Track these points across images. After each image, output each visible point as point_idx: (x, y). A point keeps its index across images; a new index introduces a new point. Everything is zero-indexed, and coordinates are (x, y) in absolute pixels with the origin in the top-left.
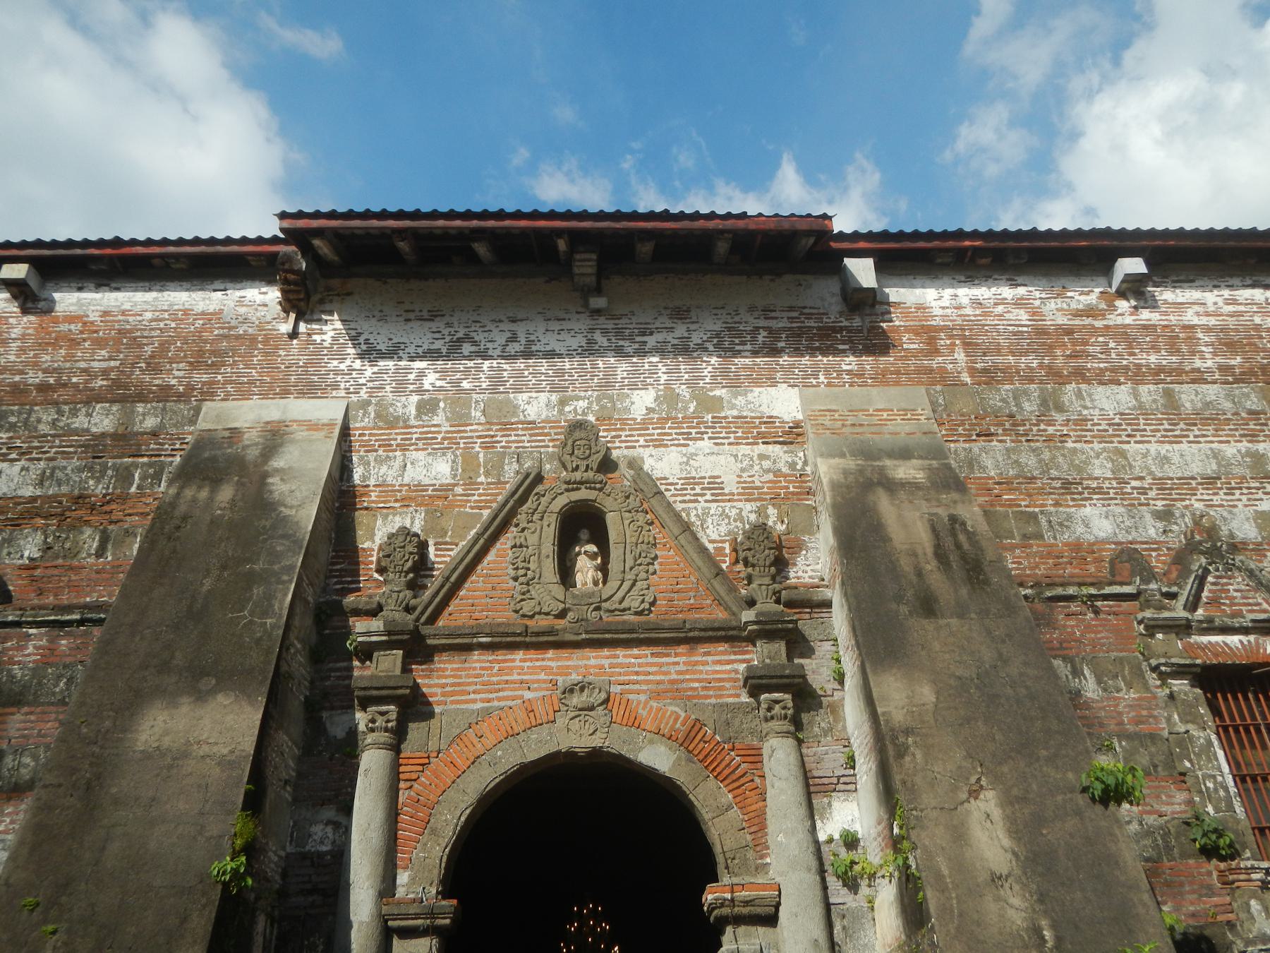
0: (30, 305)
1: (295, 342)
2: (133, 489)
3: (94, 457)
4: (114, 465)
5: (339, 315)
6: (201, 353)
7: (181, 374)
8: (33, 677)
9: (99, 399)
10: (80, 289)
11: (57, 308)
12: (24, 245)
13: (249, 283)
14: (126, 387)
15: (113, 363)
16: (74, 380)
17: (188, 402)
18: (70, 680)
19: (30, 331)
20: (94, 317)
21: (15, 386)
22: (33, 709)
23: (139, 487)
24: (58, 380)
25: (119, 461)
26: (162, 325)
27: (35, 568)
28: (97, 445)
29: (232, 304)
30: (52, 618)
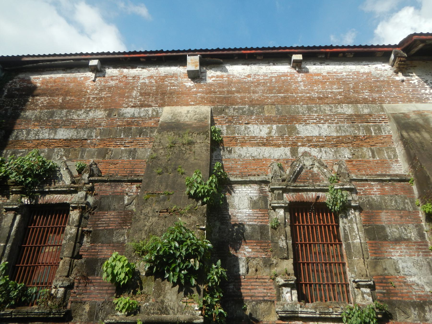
0: (299, 70)
1: (404, 83)
2: (373, 134)
3: (352, 123)
4: (361, 125)
5: (415, 74)
6: (371, 87)
7: (368, 94)
8: (381, 199)
9: (343, 103)
10: (314, 64)
11: (310, 71)
12: (297, 48)
13: (376, 63)
14: (350, 98)
15: (341, 90)
16: (330, 96)
17: (375, 103)
18: (396, 201)
19: (304, 79)
20: (325, 74)
21: (308, 97)
22: (388, 211)
23: (375, 133)
24: (324, 95)
25: (362, 124)
26: (351, 77)
27: (352, 161)
28: (351, 118)
29: (374, 70)
30: (380, 178)
